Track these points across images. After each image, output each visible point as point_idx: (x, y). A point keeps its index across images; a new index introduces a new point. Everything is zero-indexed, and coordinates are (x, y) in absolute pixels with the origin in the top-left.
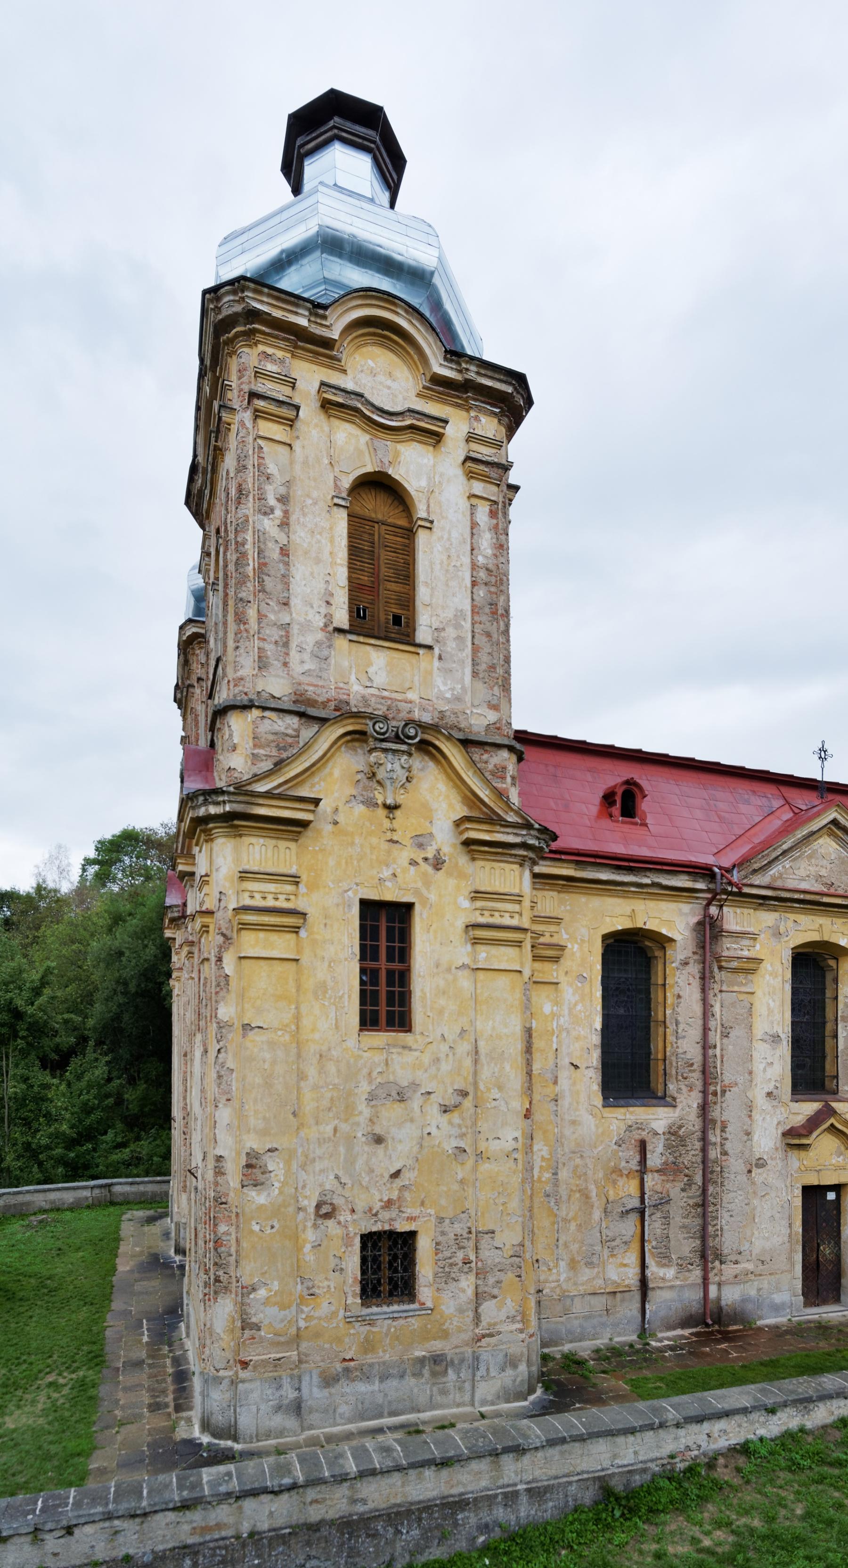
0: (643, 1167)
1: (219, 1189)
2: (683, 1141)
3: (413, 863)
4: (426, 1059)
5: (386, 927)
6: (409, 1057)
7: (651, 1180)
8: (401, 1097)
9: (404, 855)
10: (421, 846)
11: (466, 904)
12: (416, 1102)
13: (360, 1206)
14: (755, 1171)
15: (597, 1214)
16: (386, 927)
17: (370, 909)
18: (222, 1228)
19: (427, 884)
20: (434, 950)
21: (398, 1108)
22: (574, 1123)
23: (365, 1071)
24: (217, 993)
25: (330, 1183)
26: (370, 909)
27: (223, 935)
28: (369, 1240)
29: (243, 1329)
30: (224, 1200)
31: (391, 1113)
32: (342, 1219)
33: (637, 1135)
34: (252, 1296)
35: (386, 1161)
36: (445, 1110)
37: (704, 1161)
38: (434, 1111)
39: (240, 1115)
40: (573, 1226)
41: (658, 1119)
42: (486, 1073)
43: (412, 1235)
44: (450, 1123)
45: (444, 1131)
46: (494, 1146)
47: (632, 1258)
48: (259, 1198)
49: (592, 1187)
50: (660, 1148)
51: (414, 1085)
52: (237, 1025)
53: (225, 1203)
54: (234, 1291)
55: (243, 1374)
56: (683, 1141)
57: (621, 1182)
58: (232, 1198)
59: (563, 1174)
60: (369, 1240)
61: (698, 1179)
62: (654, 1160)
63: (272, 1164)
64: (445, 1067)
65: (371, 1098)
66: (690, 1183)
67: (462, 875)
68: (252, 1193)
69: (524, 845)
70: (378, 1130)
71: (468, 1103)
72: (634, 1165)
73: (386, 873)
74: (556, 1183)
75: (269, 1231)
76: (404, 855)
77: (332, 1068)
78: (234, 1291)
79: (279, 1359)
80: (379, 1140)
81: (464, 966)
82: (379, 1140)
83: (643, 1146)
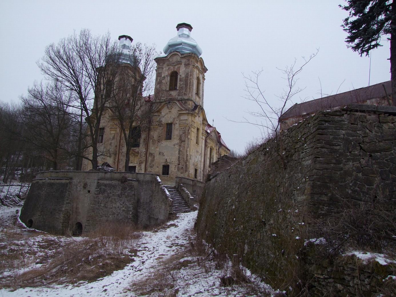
39: (190, 149)
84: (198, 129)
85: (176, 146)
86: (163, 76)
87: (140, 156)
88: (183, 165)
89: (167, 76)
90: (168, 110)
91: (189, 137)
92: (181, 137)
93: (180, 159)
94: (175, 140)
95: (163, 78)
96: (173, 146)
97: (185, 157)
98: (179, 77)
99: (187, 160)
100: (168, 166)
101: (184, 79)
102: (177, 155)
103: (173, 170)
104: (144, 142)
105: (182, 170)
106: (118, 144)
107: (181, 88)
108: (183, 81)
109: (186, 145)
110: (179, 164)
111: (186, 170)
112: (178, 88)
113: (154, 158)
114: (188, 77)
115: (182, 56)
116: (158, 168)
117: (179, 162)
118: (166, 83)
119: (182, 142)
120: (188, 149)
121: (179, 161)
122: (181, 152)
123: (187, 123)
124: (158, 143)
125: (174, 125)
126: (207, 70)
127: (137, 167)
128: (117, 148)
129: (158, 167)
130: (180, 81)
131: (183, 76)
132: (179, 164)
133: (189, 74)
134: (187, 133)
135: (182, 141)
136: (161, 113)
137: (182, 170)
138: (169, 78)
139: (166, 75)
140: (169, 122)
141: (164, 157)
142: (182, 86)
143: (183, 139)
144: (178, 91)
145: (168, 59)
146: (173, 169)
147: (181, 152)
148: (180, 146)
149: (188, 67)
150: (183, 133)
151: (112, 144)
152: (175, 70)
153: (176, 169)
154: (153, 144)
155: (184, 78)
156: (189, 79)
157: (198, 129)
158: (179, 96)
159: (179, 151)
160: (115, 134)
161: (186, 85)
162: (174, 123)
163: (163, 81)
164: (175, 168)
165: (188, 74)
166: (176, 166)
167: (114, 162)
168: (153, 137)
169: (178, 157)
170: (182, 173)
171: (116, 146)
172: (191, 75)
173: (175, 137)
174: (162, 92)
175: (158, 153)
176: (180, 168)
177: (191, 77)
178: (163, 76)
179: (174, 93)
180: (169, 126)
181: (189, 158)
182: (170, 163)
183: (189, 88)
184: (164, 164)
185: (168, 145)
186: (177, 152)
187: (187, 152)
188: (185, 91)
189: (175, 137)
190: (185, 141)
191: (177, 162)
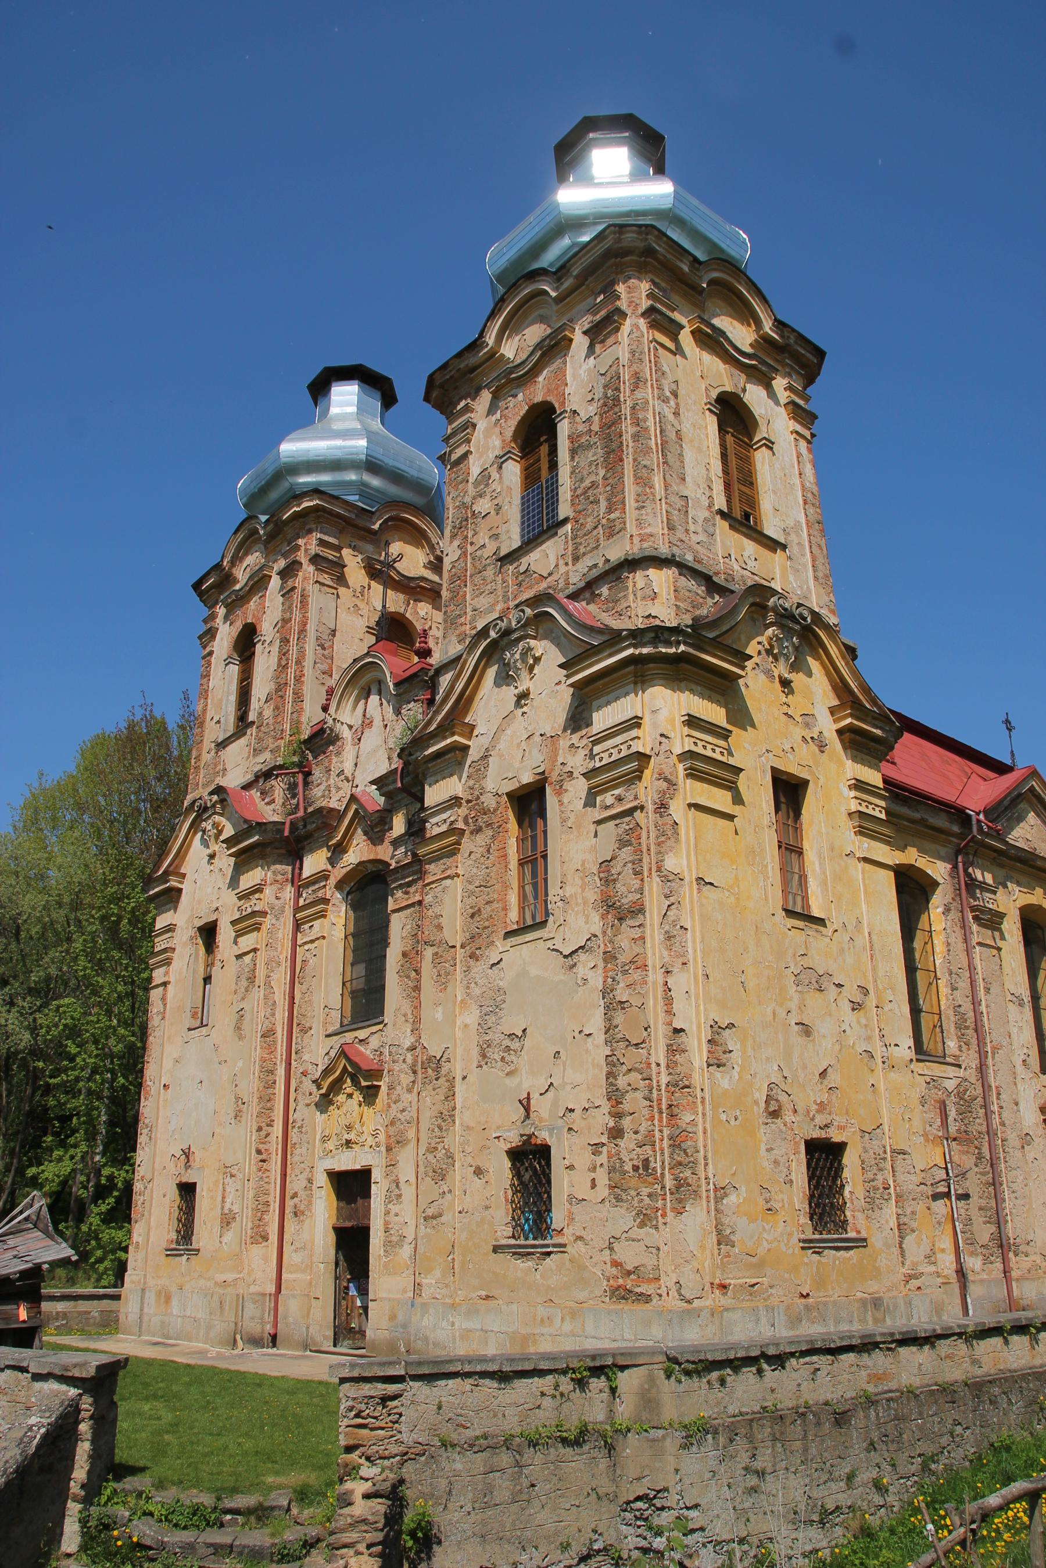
1: (679, 1069)
18: (687, 1117)
23: (791, 952)
24: (659, 844)
27: (666, 779)
29: (719, 1243)
30: (687, 1083)
31: (814, 1000)
32: (787, 1119)
34: (724, 1201)
38: (848, 1006)
44: (858, 1022)
48: (724, 1081)
52: (690, 877)
53: (688, 1087)
54: (704, 1194)
55: (726, 1301)
58: (696, 1080)
63: (731, 1040)
64: (849, 959)
68: (717, 1073)
75: (733, 1122)
78: (704, 1194)
79: (753, 1286)
84: (789, 791)
85: (581, 971)
86: (475, 471)
87: (391, 1088)
88: (648, 1141)
89: (500, 462)
90: (509, 693)
91: (671, 863)
92: (608, 881)
93: (622, 1082)
94: (577, 920)
95: (477, 483)
96: (560, 976)
97: (659, 1054)
98: (564, 429)
99: (680, 1085)
100: (544, 1152)
101: (596, 427)
102: (598, 1050)
103: (582, 1191)
104: (402, 973)
105: (645, 1191)
106: (281, 1015)
107: (584, 496)
108: (589, 446)
109: (655, 952)
110: (616, 1133)
111: (680, 1184)
112: (564, 510)
113: (450, 1096)
114: (616, 401)
115: (568, 283)
116: (478, 1183)
117: (618, 1116)
118: (498, 508)
119: (621, 919)
120: (679, 982)
121: (615, 1096)
122: (619, 1018)
123: (637, 747)
124: (468, 970)
125: (560, 791)
126: (821, 354)
127: (376, 1175)
128: (271, 1049)
129: (478, 1172)
130: (573, 452)
131: (588, 410)
132: (616, 1133)
133: (626, 375)
134: (648, 838)
135: (621, 912)
136: (472, 727)
137: (645, 1191)
138: (513, 471)
139: (491, 455)
140: (527, 778)
141: (511, 1082)
142: (587, 483)
143: (625, 890)
144: (569, 527)
145: (492, 354)
146: (571, 1180)
147: (619, 1018)
148: (609, 957)
149: (610, 341)
150: (622, 843)
151: (246, 1025)
152: (538, 398)
153: (602, 1178)
154: (443, 980)
155: (597, 418)
156: (626, 410)
157: (789, 791)
158: (576, 559)
159: (613, 1006)
160: (255, 950)
161: (613, 457)
162: (554, 777)
163: (483, 506)
164: (594, 1169)
165: (613, 383)
166: (596, 1148)
167: (259, 1152)
168: (439, 927)
169: (605, 1069)
170: (645, 1219)
171: (268, 1034)
172: (638, 381)
173: (569, 891)
174: (477, 579)
175: (475, 1052)
176: (628, 1167)
177: (648, 393)
178: (475, 471)
179: (546, 557)
180: (529, 802)
181: (697, 1053)
182: (551, 1130)
183: (639, 480)
184: (514, 1139)
185: (534, 971)
186: (596, 1023)
187: (669, 1012)
188: (610, 510)
189: (569, 891)
190: (638, 910)
191: (602, 1119)
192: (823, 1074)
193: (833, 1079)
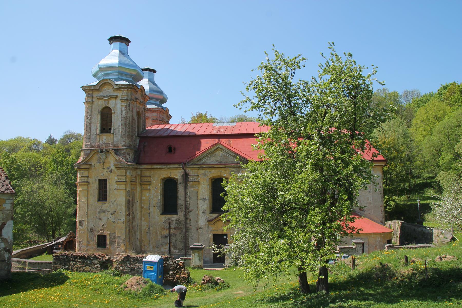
0: (170, 228)
2: (180, 222)
3: (107, 172)
4: (109, 205)
5: (103, 183)
6: (106, 205)
7: (171, 231)
8: (104, 212)
9: (105, 171)
10: (108, 169)
11: (116, 178)
12: (107, 213)
13: (97, 230)
14: (199, 230)
15: (159, 237)
16: (103, 183)
17: (100, 180)
19: (109, 175)
20: (111, 186)
21: (104, 214)
22: (154, 218)
25: (92, 226)
26: (100, 180)
28: (99, 236)
31: (103, 214)
33: (168, 221)
35: (101, 223)
36: (112, 214)
37: (186, 227)
40: (153, 239)
41: (174, 217)
42: (118, 208)
43: (106, 236)
45: (111, 218)
46: (120, 221)
47: (167, 247)
49: (158, 232)
50: (174, 224)
51: (106, 210)
56: (180, 222)
57: (165, 231)
59: (151, 228)
60: (99, 236)
61: (184, 231)
62: (173, 226)
64: (112, 207)
65: (99, 212)
66: (182, 232)
67: (115, 173)
69: (124, 167)
70: (100, 218)
71: (116, 213)
72: (168, 227)
73: (102, 174)
74: (150, 230)
76: (105, 171)
77: (93, 207)
80: (100, 219)
81: (115, 189)
82: (100, 219)
83: (170, 223)
192: (103, 225)
193: (105, 226)
